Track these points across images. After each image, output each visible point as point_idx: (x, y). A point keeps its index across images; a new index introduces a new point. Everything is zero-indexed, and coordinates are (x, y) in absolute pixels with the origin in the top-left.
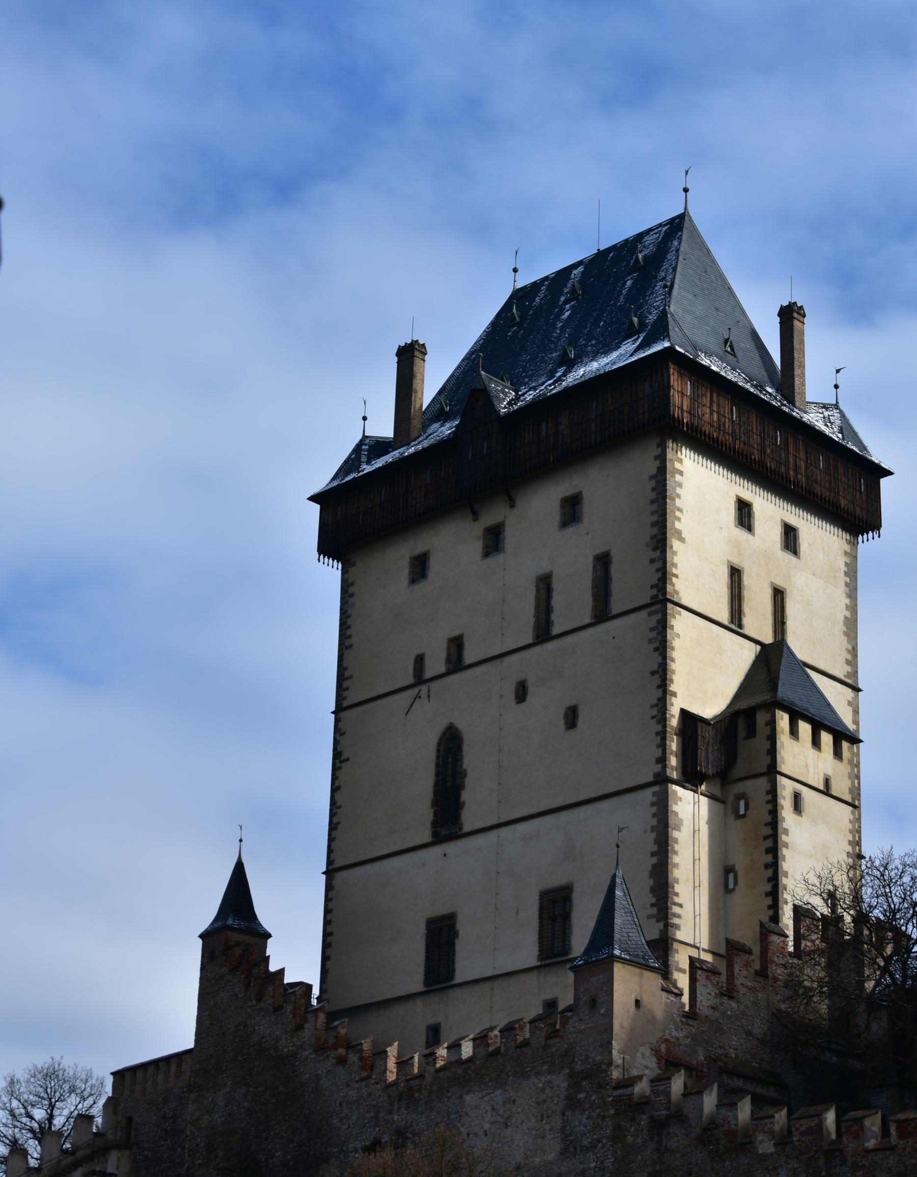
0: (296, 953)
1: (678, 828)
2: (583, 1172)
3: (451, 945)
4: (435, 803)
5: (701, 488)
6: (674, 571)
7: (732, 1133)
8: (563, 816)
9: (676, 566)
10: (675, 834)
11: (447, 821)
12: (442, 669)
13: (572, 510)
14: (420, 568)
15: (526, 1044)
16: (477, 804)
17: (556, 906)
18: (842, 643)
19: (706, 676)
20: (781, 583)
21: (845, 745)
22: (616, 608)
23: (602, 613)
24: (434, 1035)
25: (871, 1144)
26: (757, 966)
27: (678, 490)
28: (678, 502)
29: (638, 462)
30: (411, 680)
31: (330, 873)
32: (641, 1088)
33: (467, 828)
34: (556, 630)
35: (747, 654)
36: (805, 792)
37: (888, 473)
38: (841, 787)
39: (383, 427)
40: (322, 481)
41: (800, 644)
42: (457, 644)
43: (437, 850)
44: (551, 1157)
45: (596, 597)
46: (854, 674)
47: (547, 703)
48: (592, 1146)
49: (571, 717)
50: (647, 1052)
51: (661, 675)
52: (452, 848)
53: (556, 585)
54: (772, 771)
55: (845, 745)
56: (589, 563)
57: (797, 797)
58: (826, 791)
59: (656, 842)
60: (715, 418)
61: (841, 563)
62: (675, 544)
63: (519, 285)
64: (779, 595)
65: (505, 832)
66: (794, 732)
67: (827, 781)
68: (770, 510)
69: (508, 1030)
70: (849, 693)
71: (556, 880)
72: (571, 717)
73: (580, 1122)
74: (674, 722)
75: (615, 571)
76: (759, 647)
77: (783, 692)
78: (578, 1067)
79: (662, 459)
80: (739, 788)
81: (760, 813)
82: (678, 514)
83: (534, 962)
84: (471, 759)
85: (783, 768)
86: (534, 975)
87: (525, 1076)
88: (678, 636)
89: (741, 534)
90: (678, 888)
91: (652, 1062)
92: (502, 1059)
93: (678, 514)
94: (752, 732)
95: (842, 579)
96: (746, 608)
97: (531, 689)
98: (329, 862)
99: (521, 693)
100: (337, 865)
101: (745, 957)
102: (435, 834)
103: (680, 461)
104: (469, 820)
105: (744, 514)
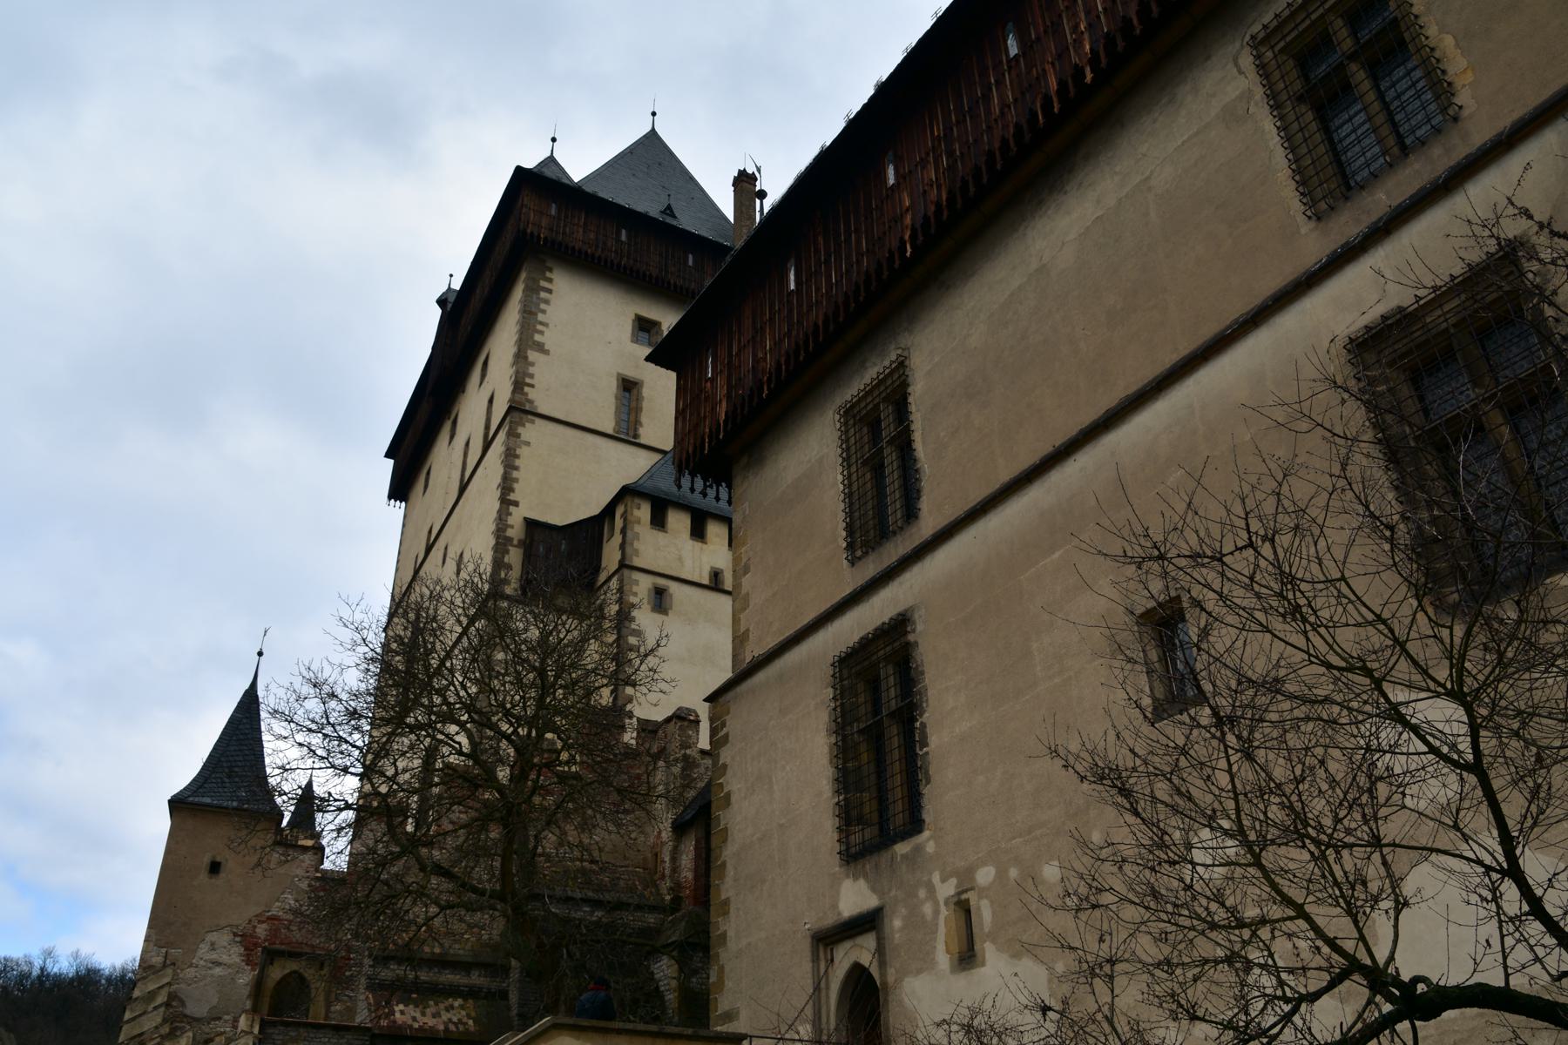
6: (528, 380)
9: (532, 376)
27: (543, 306)
28: (540, 317)
36: (674, 587)
50: (223, 938)
60: (592, 236)
62: (532, 355)
74: (516, 531)
82: (539, 327)
88: (528, 444)
93: (539, 327)
96: (644, 419)
103: (550, 280)
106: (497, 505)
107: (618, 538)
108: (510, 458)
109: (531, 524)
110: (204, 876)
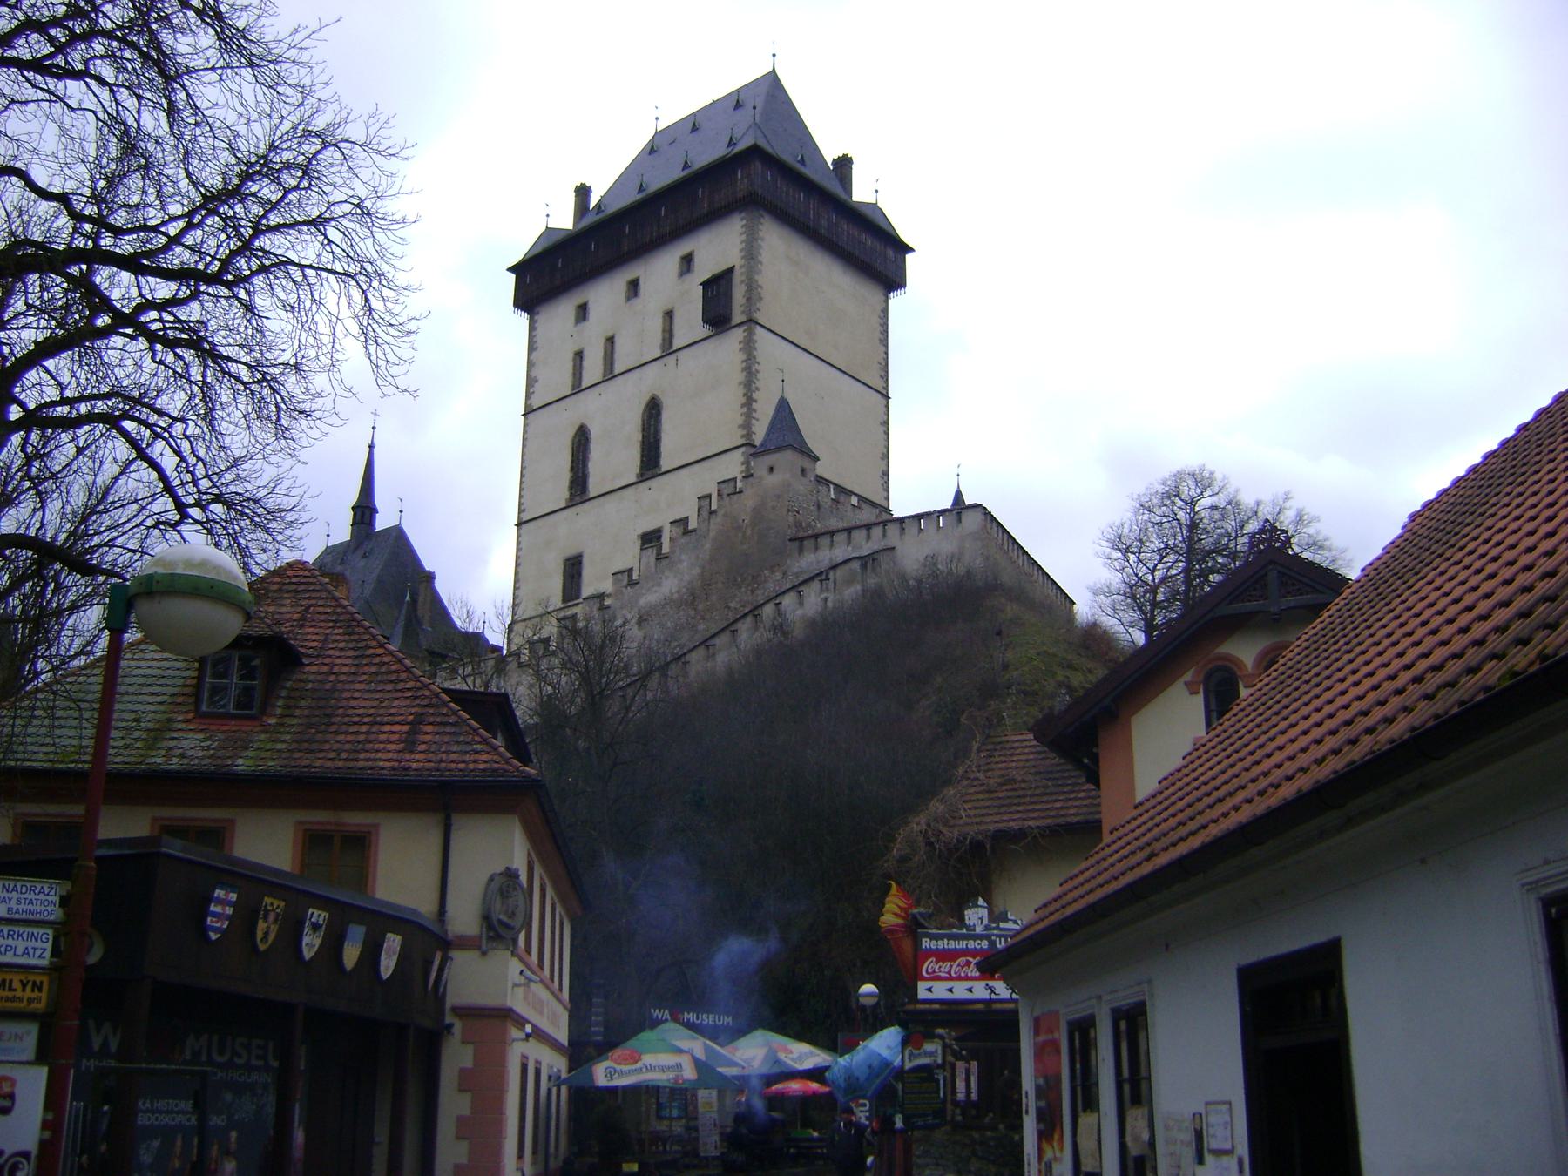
37: (910, 250)
46: (886, 388)
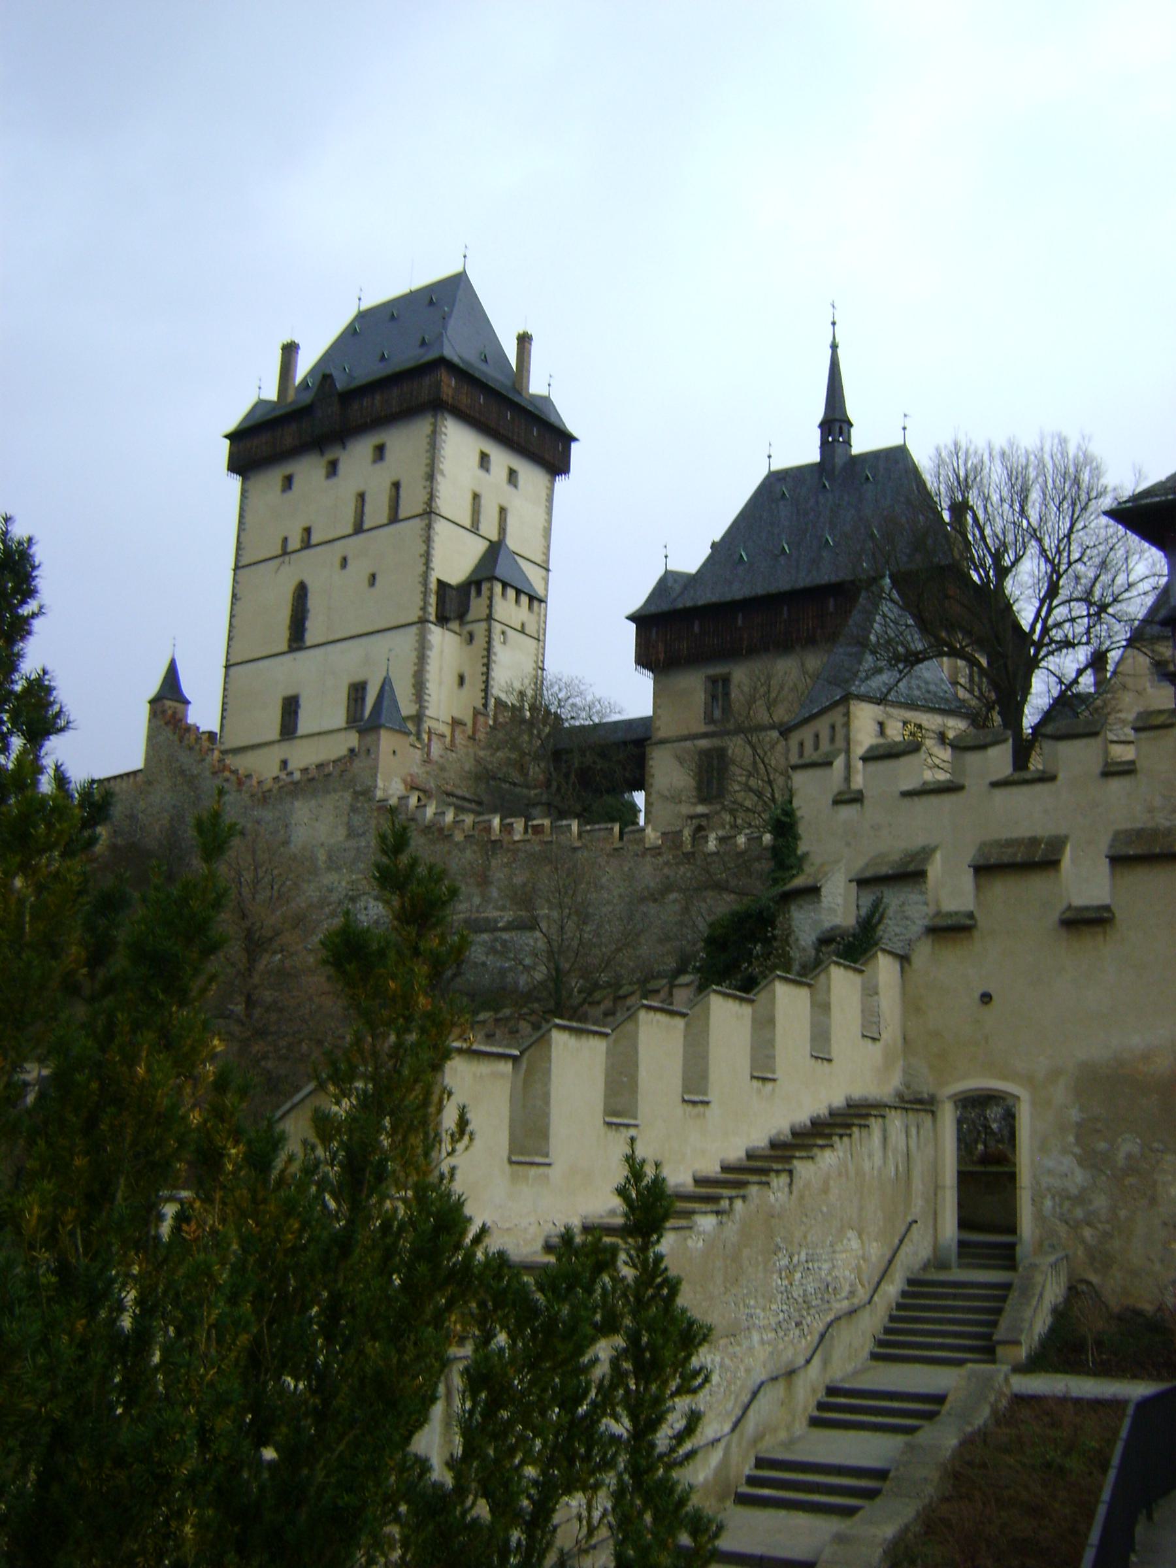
0: (204, 714)
1: (430, 649)
2: (358, 849)
3: (296, 713)
4: (290, 628)
5: (460, 445)
7: (441, 830)
8: (364, 640)
10: (428, 653)
11: (297, 637)
12: (298, 546)
13: (380, 452)
14: (288, 482)
15: (329, 775)
16: (314, 631)
17: (358, 691)
18: (541, 541)
19: (455, 558)
20: (505, 504)
21: (536, 604)
22: (402, 515)
23: (394, 519)
24: (284, 763)
25: (517, 838)
26: (470, 732)
29: (421, 428)
30: (279, 552)
31: (227, 667)
32: (393, 801)
33: (308, 643)
34: (366, 526)
35: (480, 547)
36: (509, 631)
37: (575, 439)
38: (531, 629)
39: (271, 394)
40: (232, 425)
41: (512, 543)
42: (308, 531)
43: (290, 656)
44: (341, 838)
45: (390, 508)
46: (547, 561)
47: (359, 569)
48: (364, 834)
49: (373, 578)
50: (398, 780)
51: (427, 557)
52: (300, 655)
53: (368, 499)
54: (490, 618)
55: (536, 604)
56: (387, 485)
57: (503, 633)
58: (522, 631)
59: (418, 658)
61: (544, 496)
62: (439, 478)
63: (362, 309)
64: (503, 511)
65: (330, 648)
66: (504, 594)
67: (523, 625)
68: (502, 460)
69: (320, 766)
70: (543, 572)
71: (357, 678)
72: (373, 578)
73: (357, 820)
74: (433, 586)
75: (403, 492)
76: (487, 543)
77: (500, 571)
78: (358, 788)
79: (435, 425)
80: (469, 627)
81: (480, 640)
83: (344, 725)
84: (313, 602)
85: (496, 616)
86: (342, 735)
87: (328, 792)
89: (481, 473)
90: (428, 685)
91: (401, 787)
92: (316, 781)
94: (479, 593)
95: (544, 503)
96: (482, 519)
97: (349, 561)
98: (227, 660)
99: (344, 563)
100: (231, 662)
101: (462, 727)
102: (290, 646)
104: (310, 638)
105: (484, 459)
106: (424, 568)
107: (484, 601)
108: (428, 541)
109: (439, 581)
110: (392, 756)
